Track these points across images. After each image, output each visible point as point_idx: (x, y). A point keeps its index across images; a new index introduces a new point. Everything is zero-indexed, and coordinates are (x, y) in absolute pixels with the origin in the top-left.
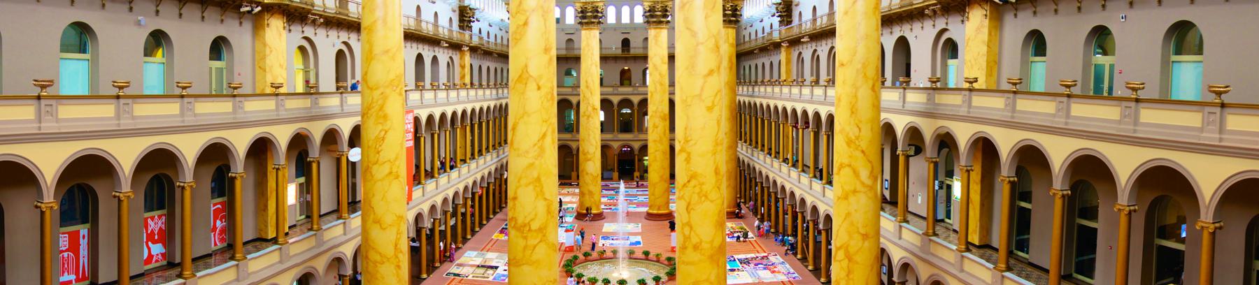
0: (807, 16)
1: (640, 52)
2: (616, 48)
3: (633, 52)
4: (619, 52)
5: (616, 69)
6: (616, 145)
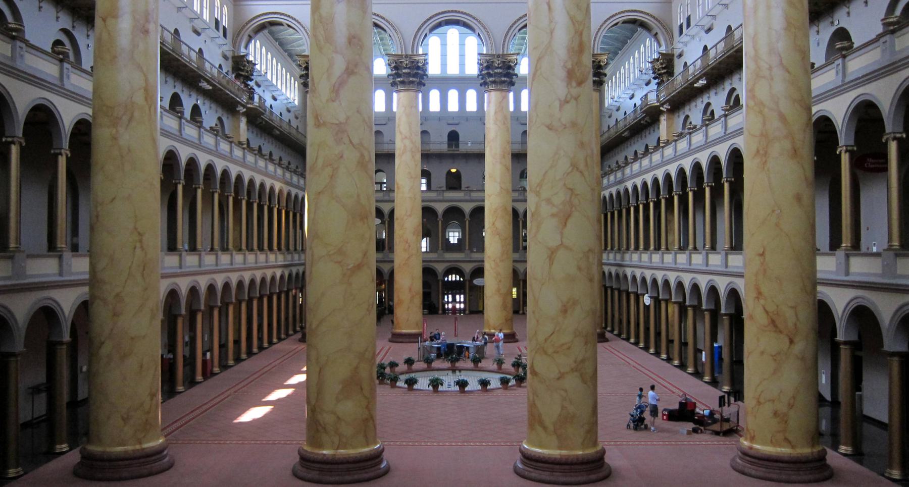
2: (440, 144)
4: (444, 148)
6: (440, 268)
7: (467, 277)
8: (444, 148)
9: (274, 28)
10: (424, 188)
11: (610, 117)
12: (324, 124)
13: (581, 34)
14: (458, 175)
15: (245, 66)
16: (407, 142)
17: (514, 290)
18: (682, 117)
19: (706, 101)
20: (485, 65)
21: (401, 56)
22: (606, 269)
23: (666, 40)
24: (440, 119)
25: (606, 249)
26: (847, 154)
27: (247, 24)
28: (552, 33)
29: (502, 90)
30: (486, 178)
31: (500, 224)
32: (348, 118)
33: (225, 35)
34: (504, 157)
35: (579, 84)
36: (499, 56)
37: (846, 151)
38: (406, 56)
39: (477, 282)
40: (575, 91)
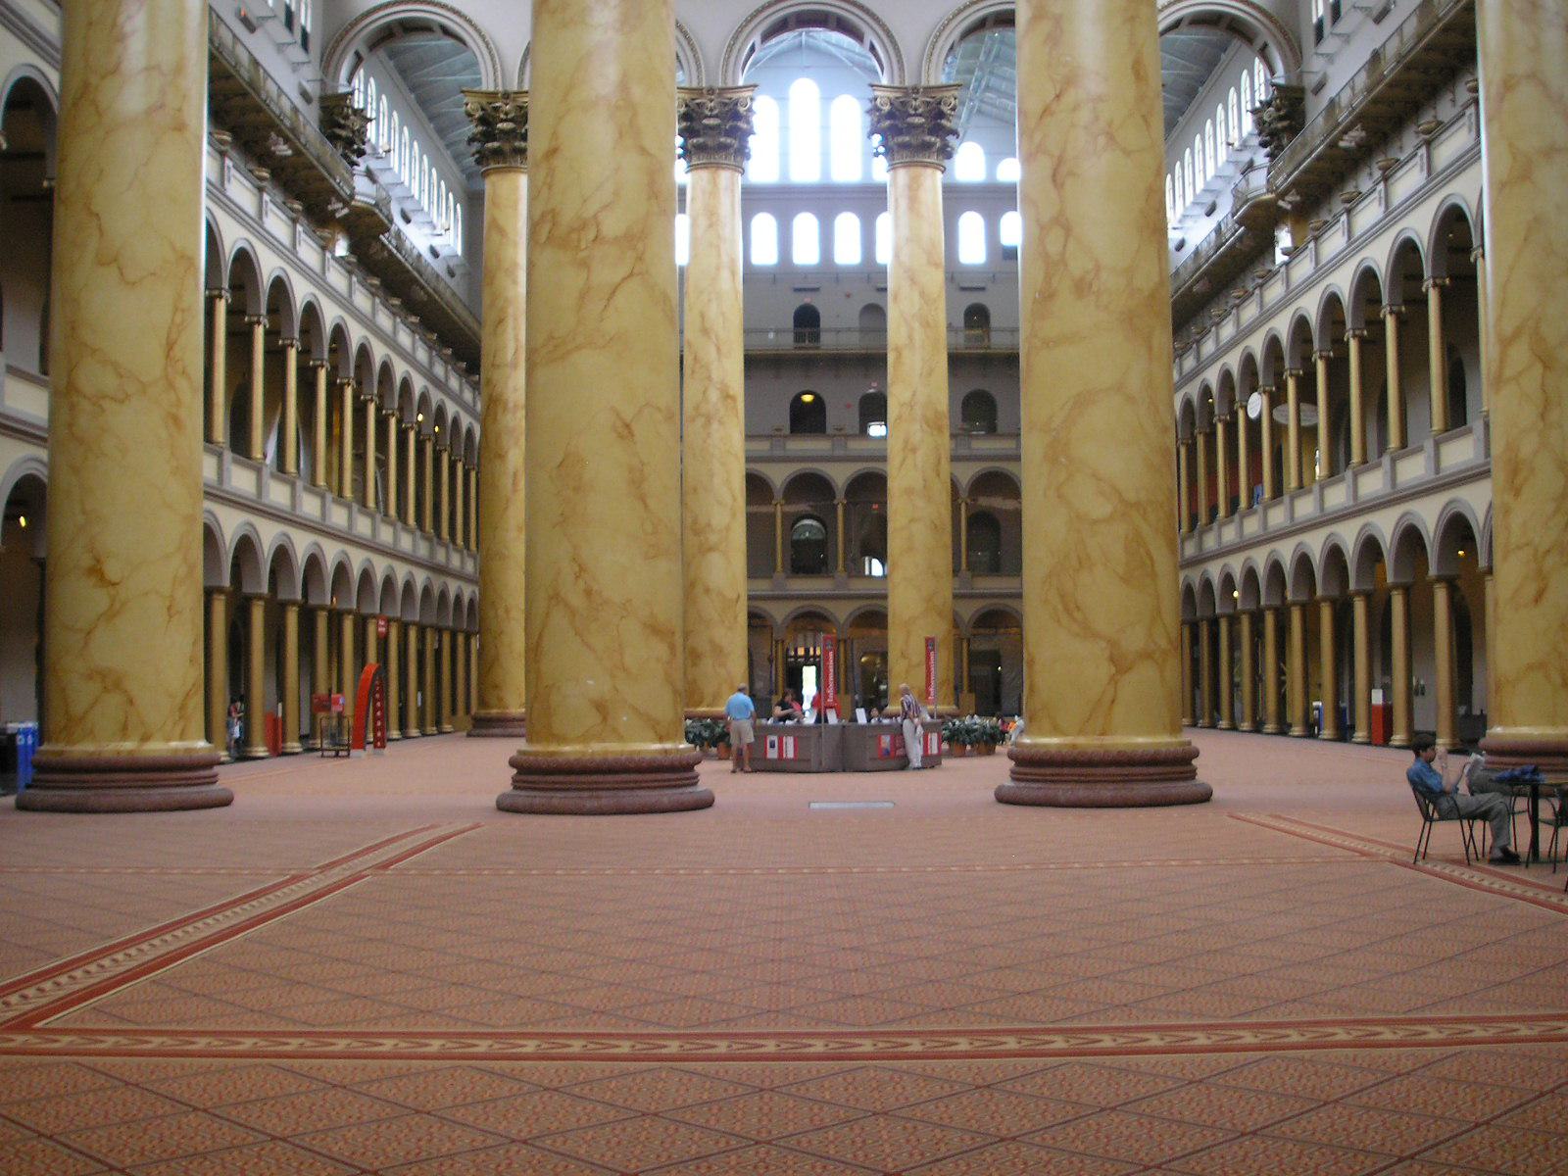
1: (852, 342)
2: (780, 338)
3: (828, 342)
4: (786, 342)
5: (782, 391)
9: (418, 41)
15: (346, 117)
20: (886, 108)
21: (699, 91)
38: (711, 91)
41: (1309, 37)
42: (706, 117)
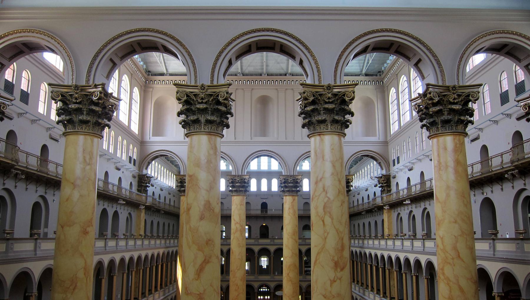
0: (403, 185)
3: (269, 213)
4: (259, 212)
5: (257, 226)
6: (256, 285)
7: (272, 291)
8: (259, 212)
10: (247, 235)
11: (354, 196)
12: (191, 294)
13: (342, 239)
14: (266, 227)
15: (145, 180)
16: (238, 226)
17: (300, 297)
18: (396, 213)
19: (410, 209)
20: (283, 181)
22: (354, 295)
23: (386, 167)
24: (256, 196)
25: (354, 281)
26: (499, 298)
27: (148, 156)
28: (325, 239)
29: (293, 196)
30: (284, 229)
31: (292, 275)
32: (205, 290)
33: (134, 164)
34: (294, 234)
35: (342, 269)
36: (291, 176)
37: (498, 296)
38: (238, 176)
39: (278, 293)
40: (339, 274)
41: (391, 164)
42: (237, 183)
